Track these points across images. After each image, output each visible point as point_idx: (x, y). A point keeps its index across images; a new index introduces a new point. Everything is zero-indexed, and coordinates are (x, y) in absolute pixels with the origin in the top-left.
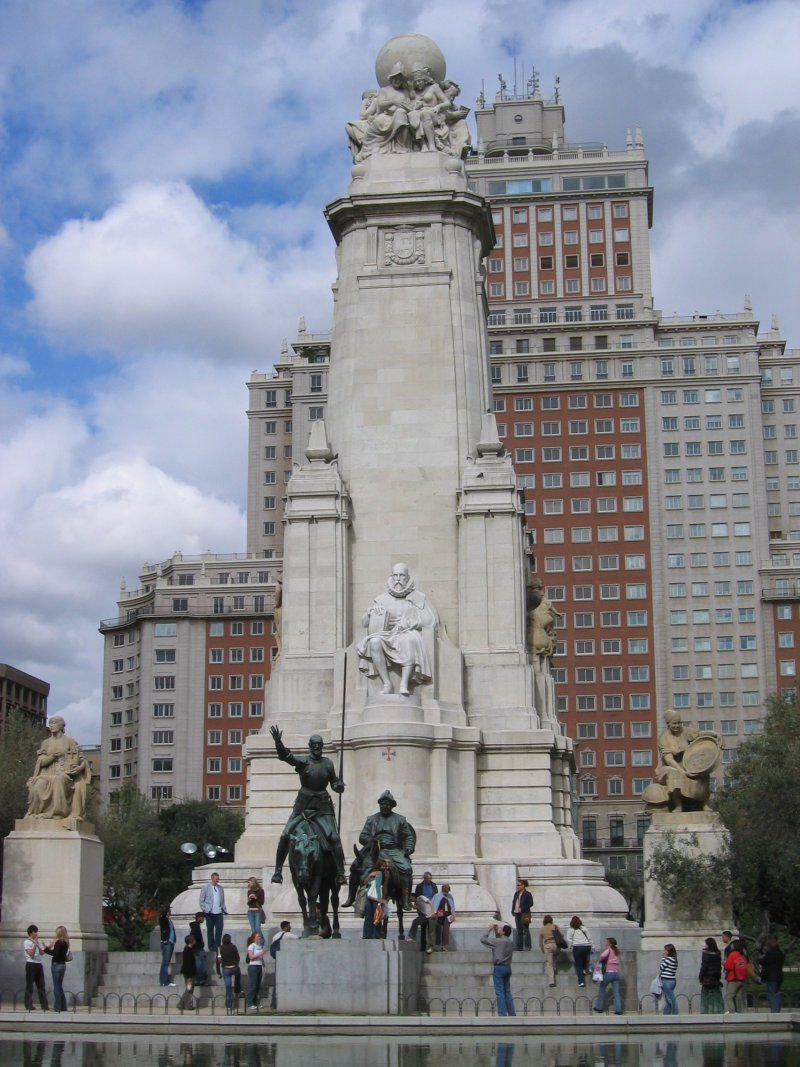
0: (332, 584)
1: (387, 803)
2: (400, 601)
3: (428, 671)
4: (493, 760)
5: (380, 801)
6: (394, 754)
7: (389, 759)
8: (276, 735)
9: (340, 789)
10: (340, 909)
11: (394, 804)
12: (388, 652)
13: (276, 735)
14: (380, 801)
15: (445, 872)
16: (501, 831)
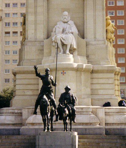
0: (41, 18)
1: (67, 89)
2: (65, 24)
3: (75, 47)
4: (95, 75)
5: (65, 89)
6: (65, 73)
7: (63, 75)
8: (36, 68)
9: (55, 85)
10: (53, 122)
11: (70, 89)
12: (62, 40)
13: (36, 68)
14: (65, 89)
15: (82, 111)
16: (98, 97)
